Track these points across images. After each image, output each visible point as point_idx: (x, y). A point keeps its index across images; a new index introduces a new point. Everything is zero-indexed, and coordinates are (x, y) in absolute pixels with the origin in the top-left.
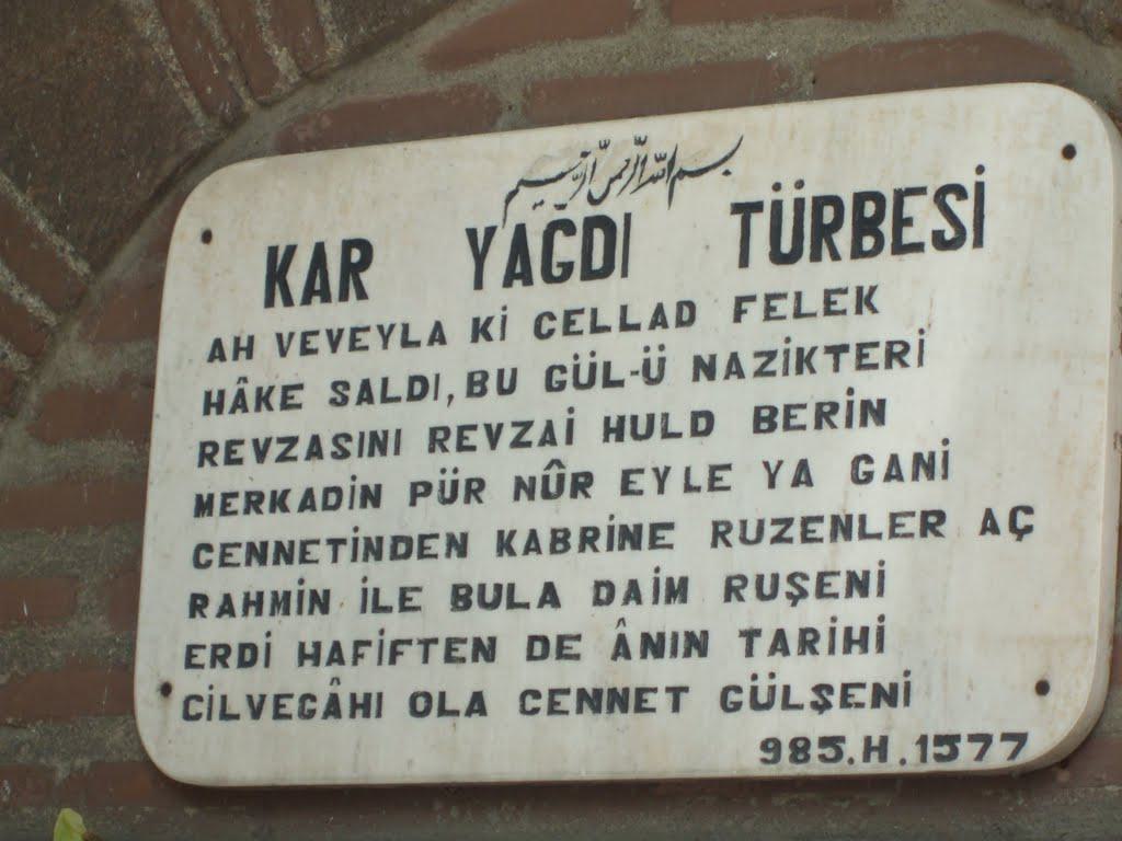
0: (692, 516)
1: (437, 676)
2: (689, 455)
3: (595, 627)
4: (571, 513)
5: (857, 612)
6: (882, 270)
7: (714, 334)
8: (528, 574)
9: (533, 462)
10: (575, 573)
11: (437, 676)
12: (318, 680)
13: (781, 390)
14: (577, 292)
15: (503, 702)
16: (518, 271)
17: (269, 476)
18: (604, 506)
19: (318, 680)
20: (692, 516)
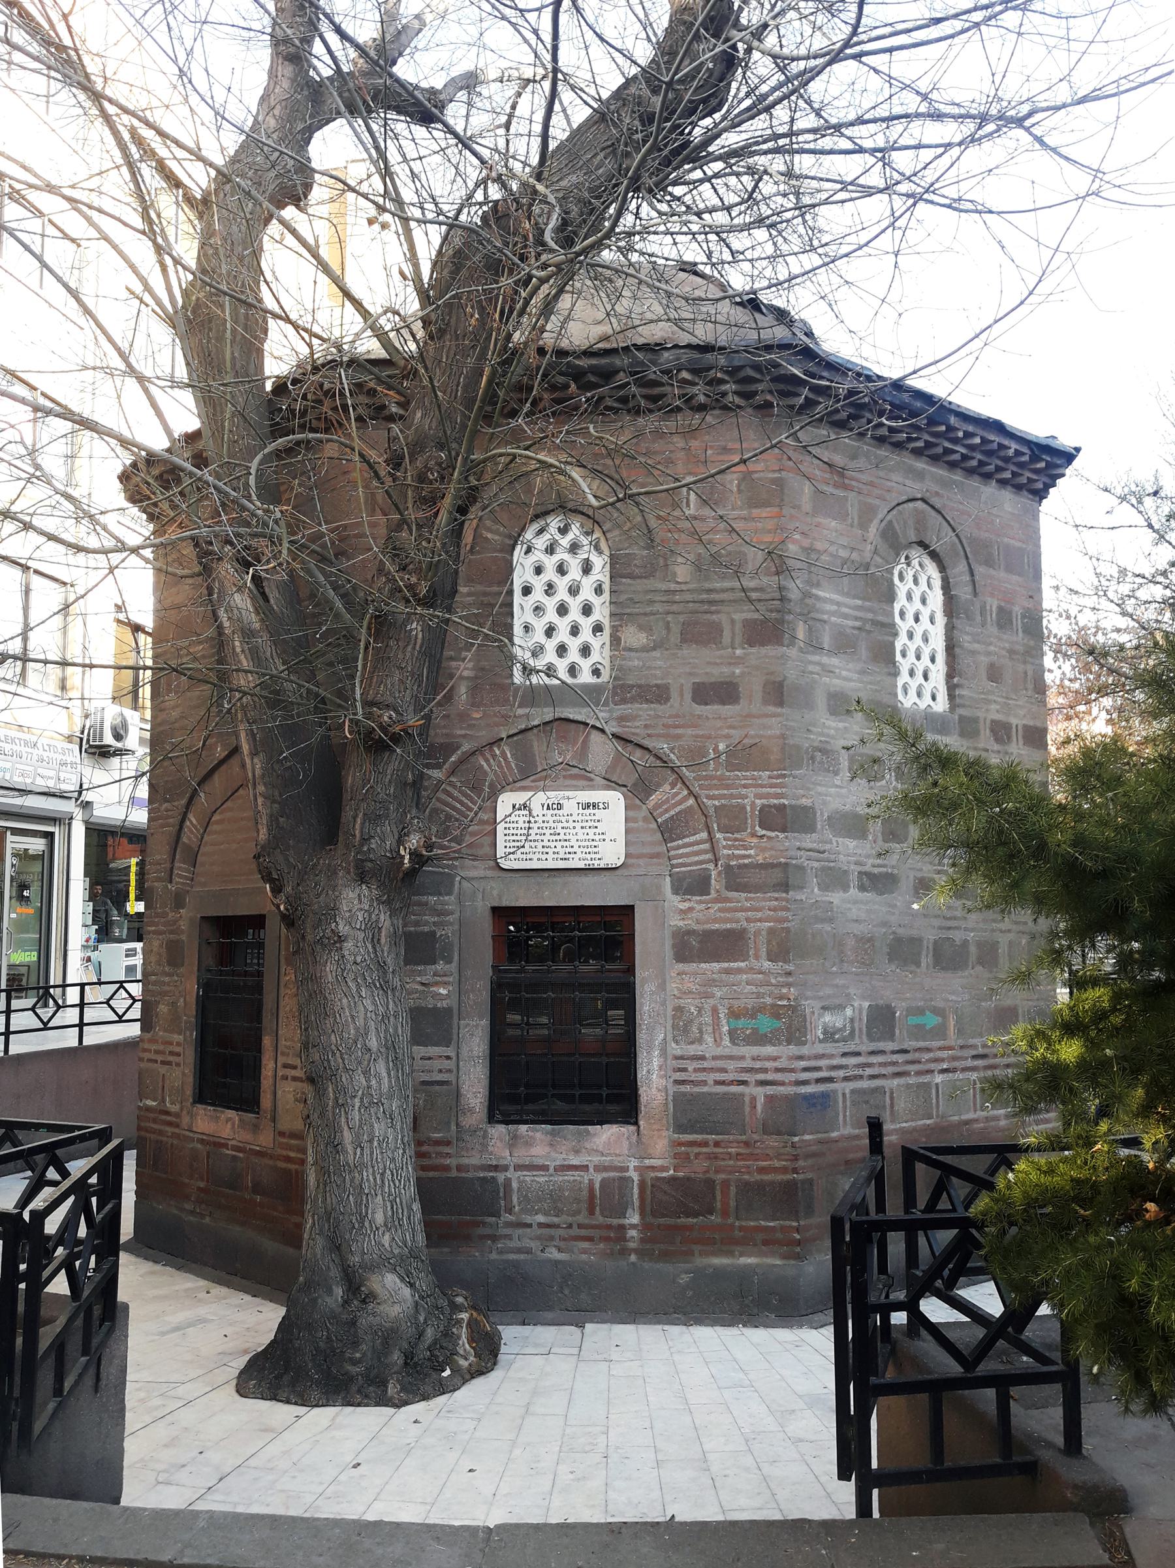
0: (574, 839)
1: (540, 856)
2: (574, 831)
3: (562, 851)
4: (557, 837)
5: (596, 850)
6: (596, 811)
7: (575, 817)
8: (552, 844)
9: (552, 831)
10: (559, 844)
11: (540, 856)
12: (524, 856)
13: (584, 824)
14: (556, 811)
15: (550, 859)
16: (548, 808)
17: (515, 832)
18: (562, 837)
19: (524, 856)
20: (574, 839)
